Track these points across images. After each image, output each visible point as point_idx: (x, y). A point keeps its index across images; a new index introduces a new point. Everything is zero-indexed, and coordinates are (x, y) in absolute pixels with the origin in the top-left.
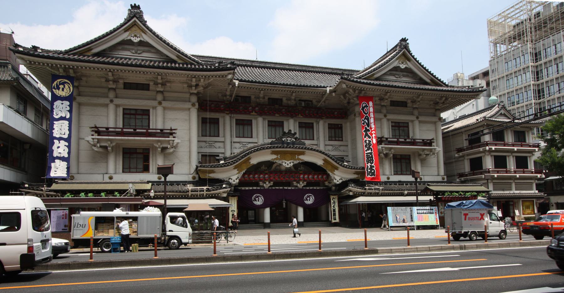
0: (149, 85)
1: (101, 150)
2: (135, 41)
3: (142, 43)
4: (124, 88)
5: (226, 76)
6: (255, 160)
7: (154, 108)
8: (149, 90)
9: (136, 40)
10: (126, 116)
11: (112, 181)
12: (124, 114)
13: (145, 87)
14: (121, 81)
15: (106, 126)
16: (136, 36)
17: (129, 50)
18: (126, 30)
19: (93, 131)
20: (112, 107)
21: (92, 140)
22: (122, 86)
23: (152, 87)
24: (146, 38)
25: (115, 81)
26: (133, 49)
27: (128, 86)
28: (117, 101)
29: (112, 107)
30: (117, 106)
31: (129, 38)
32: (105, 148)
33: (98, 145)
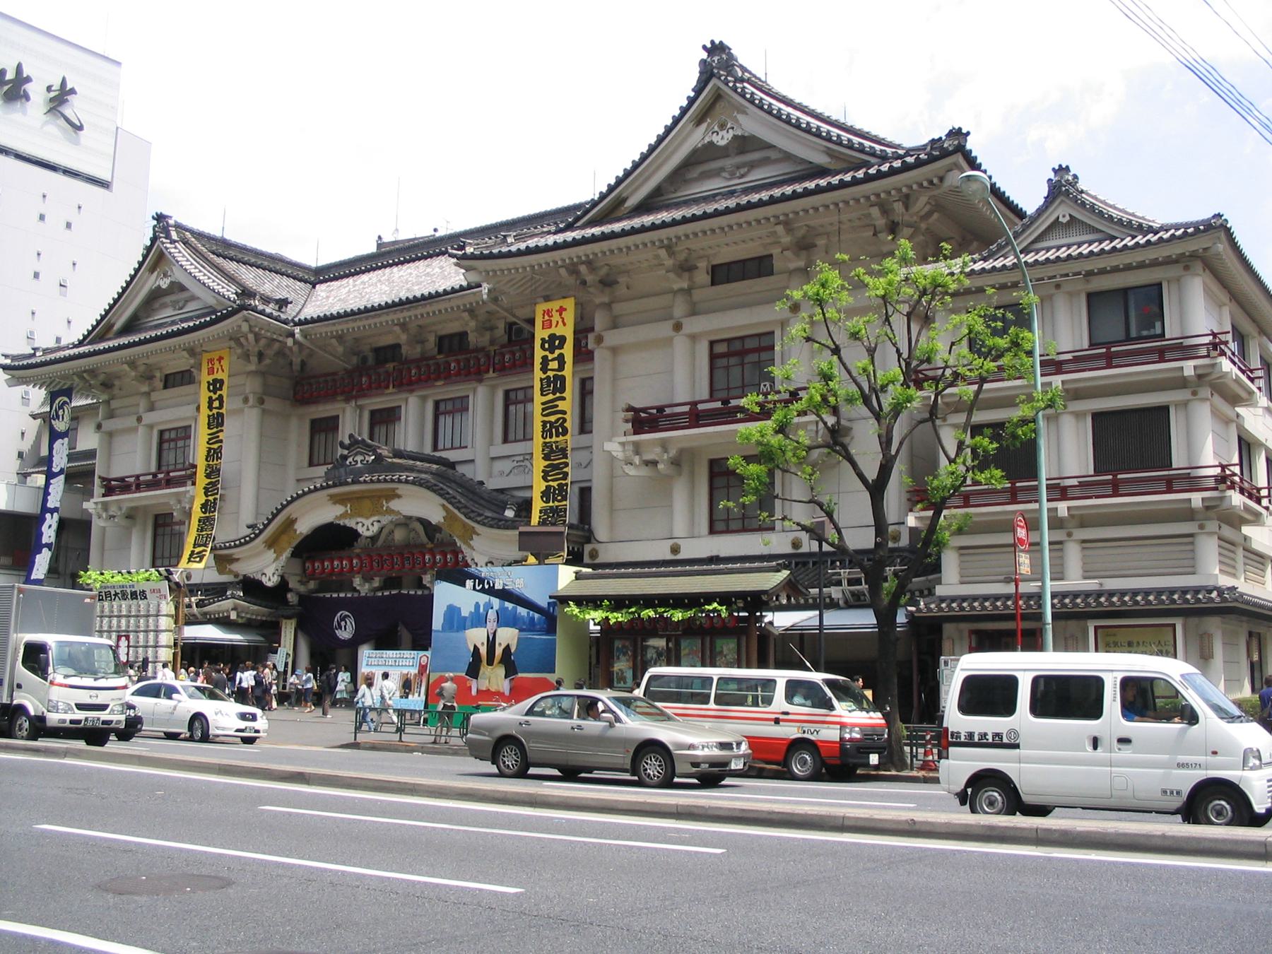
0: (771, 256)
1: (645, 472)
2: (722, 143)
3: (744, 144)
4: (713, 283)
5: (941, 179)
6: (304, 527)
7: (784, 324)
8: (771, 273)
9: (722, 139)
10: (722, 362)
11: (679, 557)
12: (713, 357)
13: (759, 267)
14: (703, 265)
15: (688, 400)
16: (722, 127)
17: (716, 173)
18: (699, 120)
19: (627, 421)
20: (680, 343)
21: (619, 448)
22: (707, 279)
23: (777, 264)
24: (751, 124)
25: (686, 268)
26: (722, 169)
27: (722, 274)
28: (694, 325)
29: (680, 343)
30: (693, 338)
31: (707, 140)
32: (653, 463)
33: (637, 460)
